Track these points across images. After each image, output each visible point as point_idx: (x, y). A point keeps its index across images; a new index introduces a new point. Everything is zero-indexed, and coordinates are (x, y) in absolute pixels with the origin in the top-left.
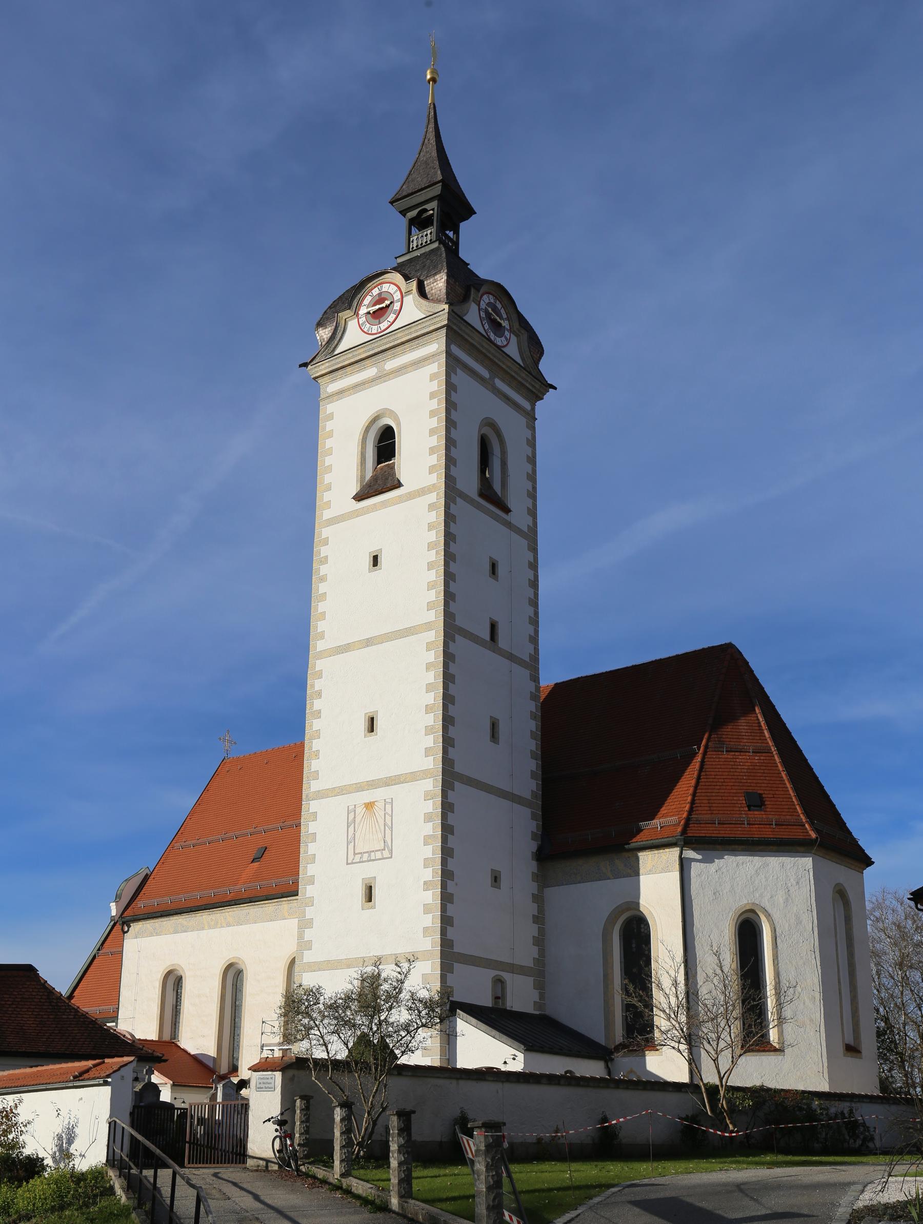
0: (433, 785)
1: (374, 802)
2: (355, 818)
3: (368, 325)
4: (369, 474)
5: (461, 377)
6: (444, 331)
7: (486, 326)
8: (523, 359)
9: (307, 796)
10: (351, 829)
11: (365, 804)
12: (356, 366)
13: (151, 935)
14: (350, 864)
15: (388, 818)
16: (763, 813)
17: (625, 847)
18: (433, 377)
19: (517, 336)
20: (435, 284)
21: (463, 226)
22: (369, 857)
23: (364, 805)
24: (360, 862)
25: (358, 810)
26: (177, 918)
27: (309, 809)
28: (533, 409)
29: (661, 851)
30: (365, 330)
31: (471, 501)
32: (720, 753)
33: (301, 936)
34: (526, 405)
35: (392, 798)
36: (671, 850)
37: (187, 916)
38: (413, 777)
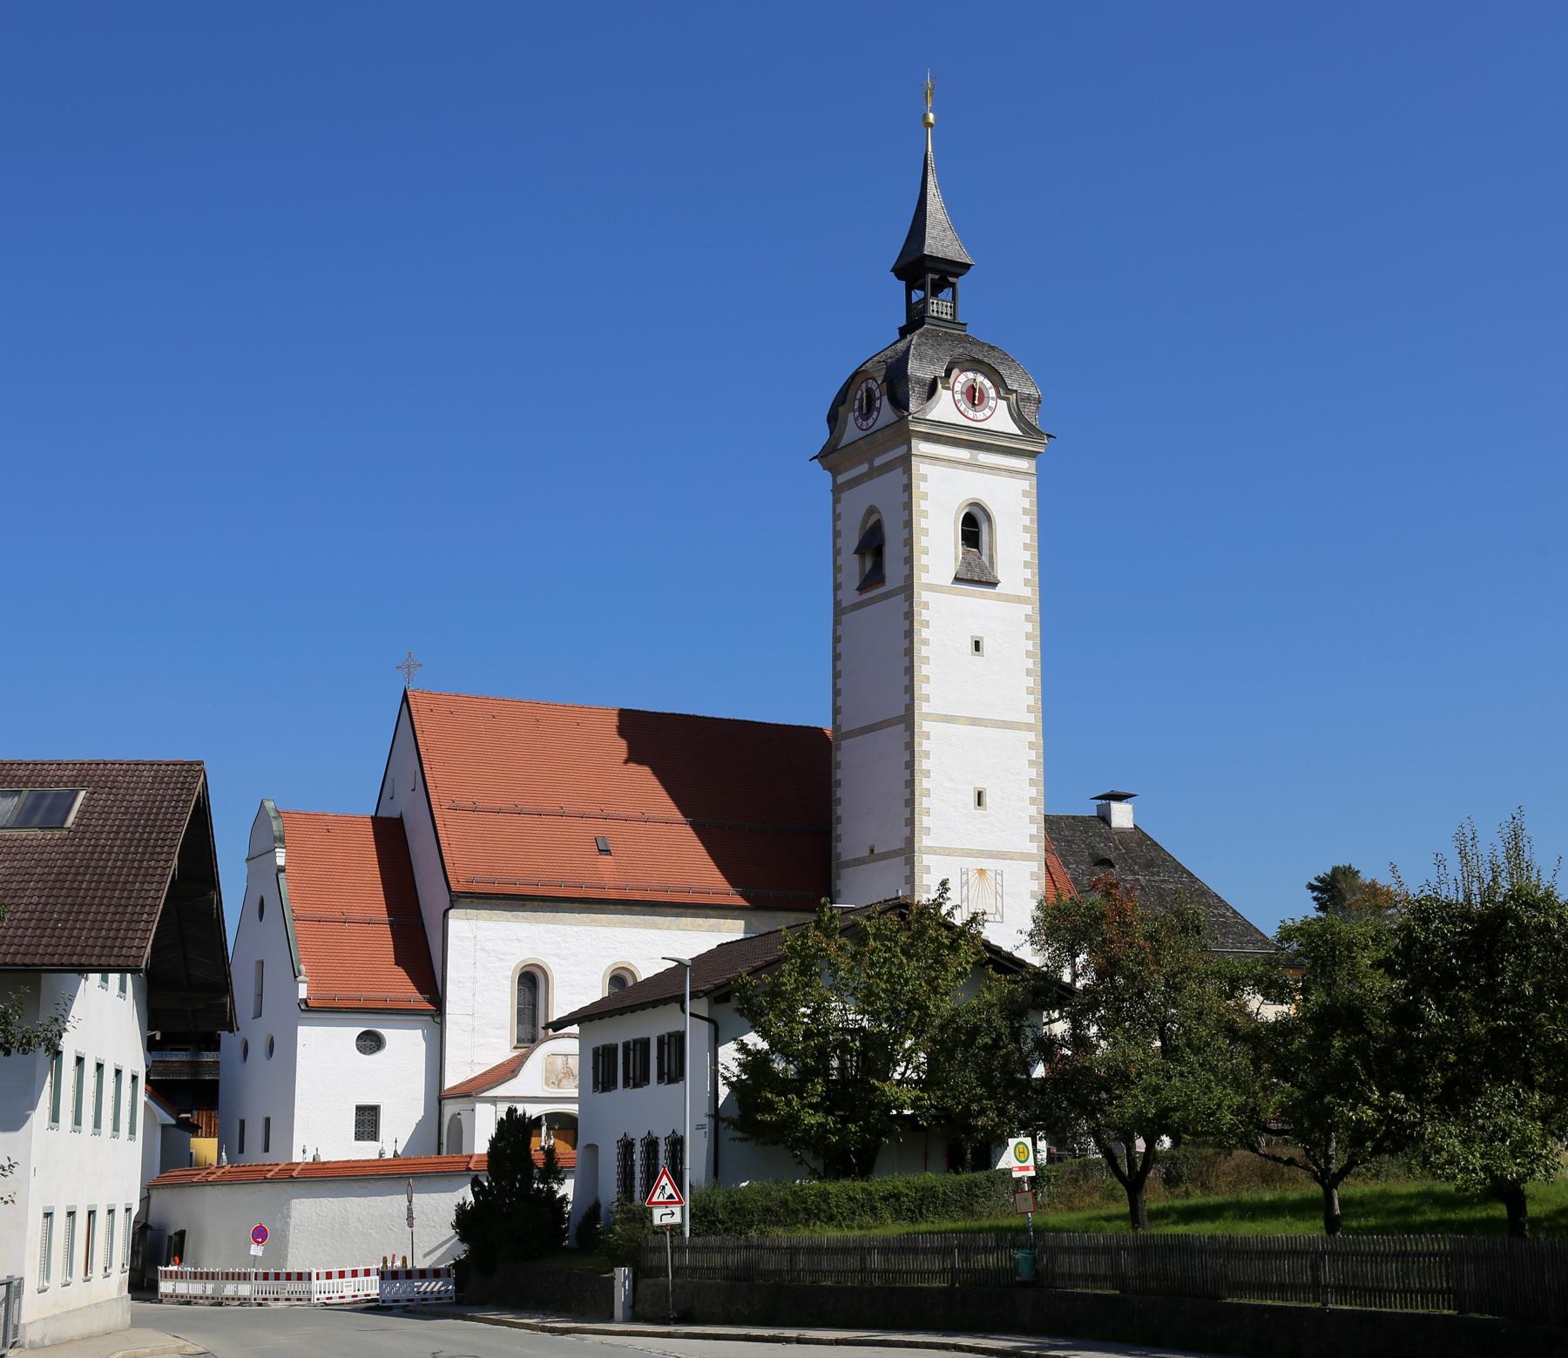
1: (985, 870)
15: (999, 888)
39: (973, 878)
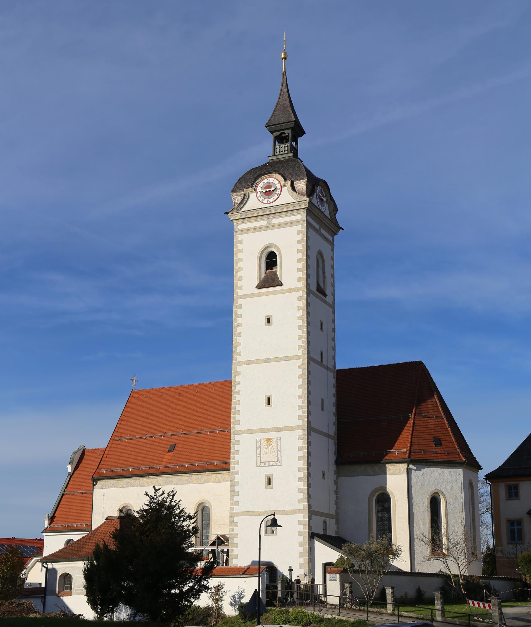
0: (303, 433)
2: (261, 445)
3: (262, 198)
4: (263, 275)
6: (305, 210)
8: (330, 216)
9: (234, 432)
10: (259, 450)
11: (266, 439)
12: (255, 218)
13: (111, 487)
14: (258, 467)
16: (441, 448)
17: (381, 462)
18: (299, 232)
19: (329, 204)
20: (300, 184)
21: (300, 139)
22: (269, 464)
23: (265, 440)
24: (264, 466)
25: (262, 442)
26: (128, 479)
27: (235, 438)
28: (333, 240)
29: (398, 464)
30: (261, 200)
32: (421, 418)
33: (232, 499)
34: (330, 238)
35: (281, 438)
36: (403, 464)
37: (134, 479)
39: (264, 442)
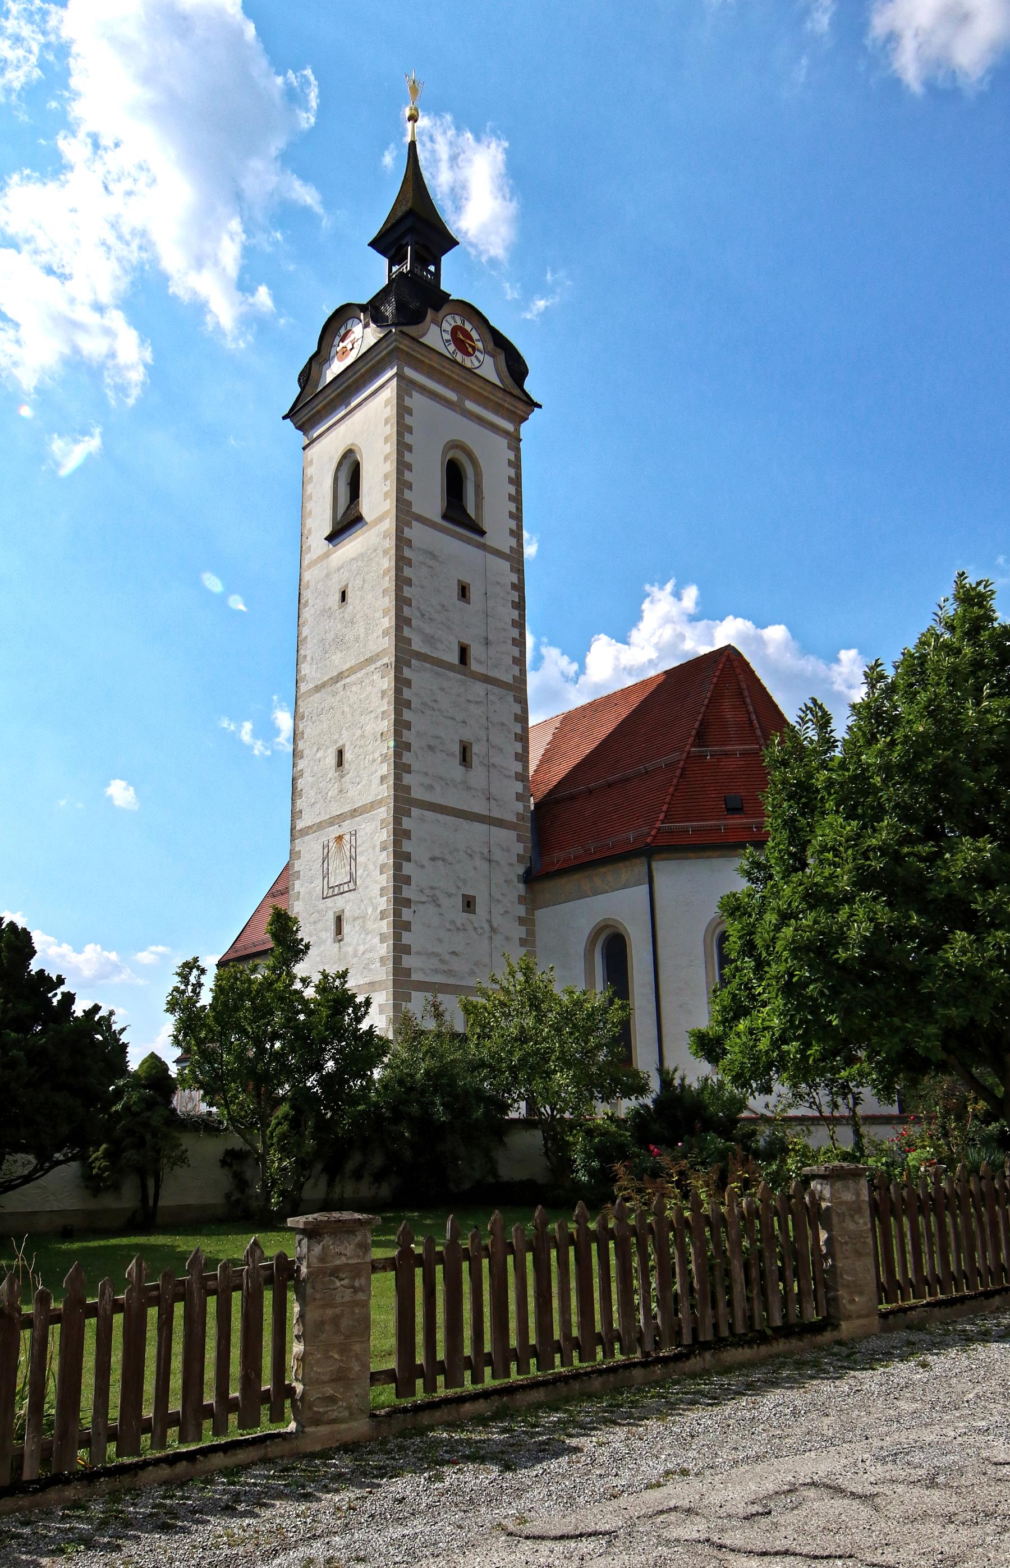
0: (385, 813)
5: (416, 401)
7: (452, 348)
8: (501, 381)
19: (493, 356)
21: (445, 260)
25: (331, 844)
28: (517, 430)
31: (433, 525)
34: (510, 427)
38: (373, 806)
